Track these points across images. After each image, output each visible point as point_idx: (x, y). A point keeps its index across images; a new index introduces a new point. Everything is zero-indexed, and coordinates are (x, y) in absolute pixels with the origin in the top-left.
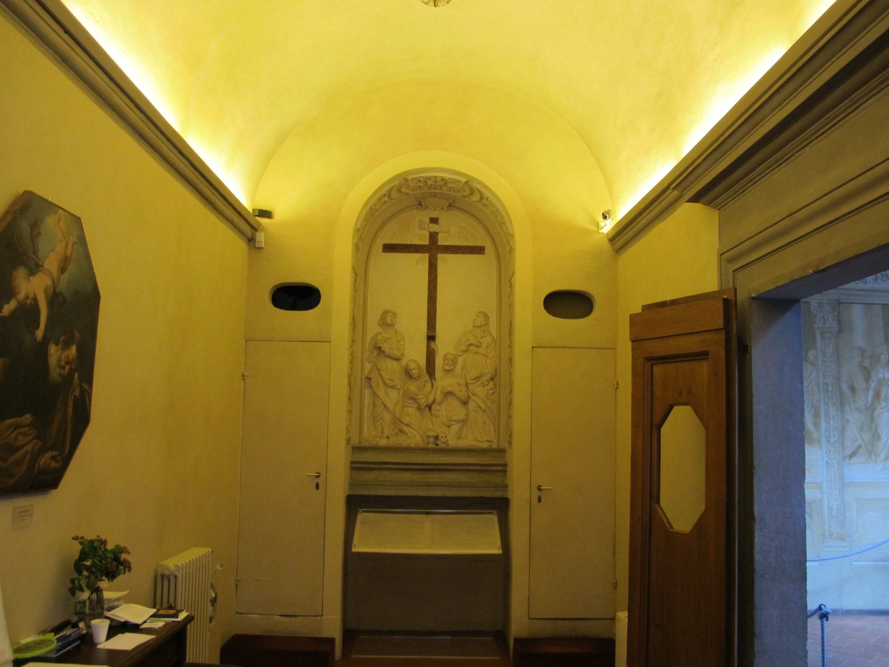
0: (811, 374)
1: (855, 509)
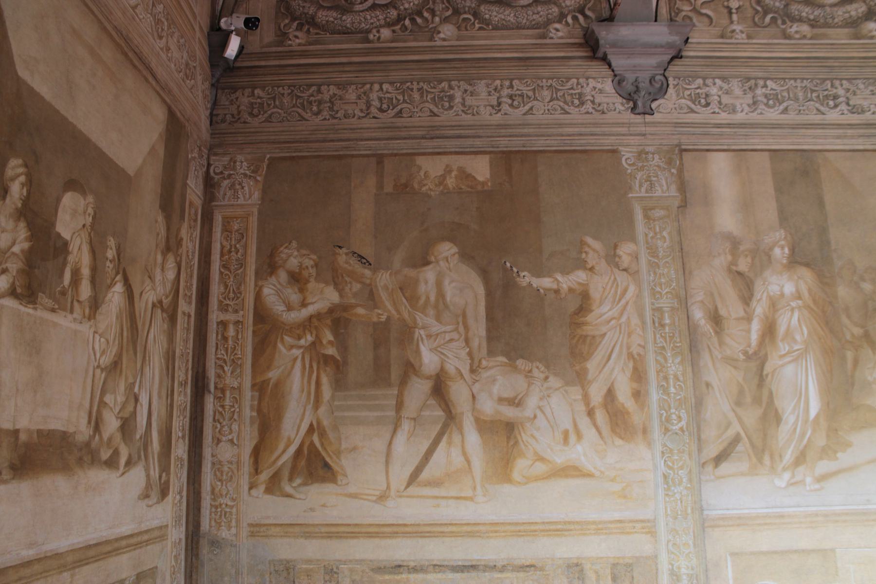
0: (625, 291)
1: (730, 574)
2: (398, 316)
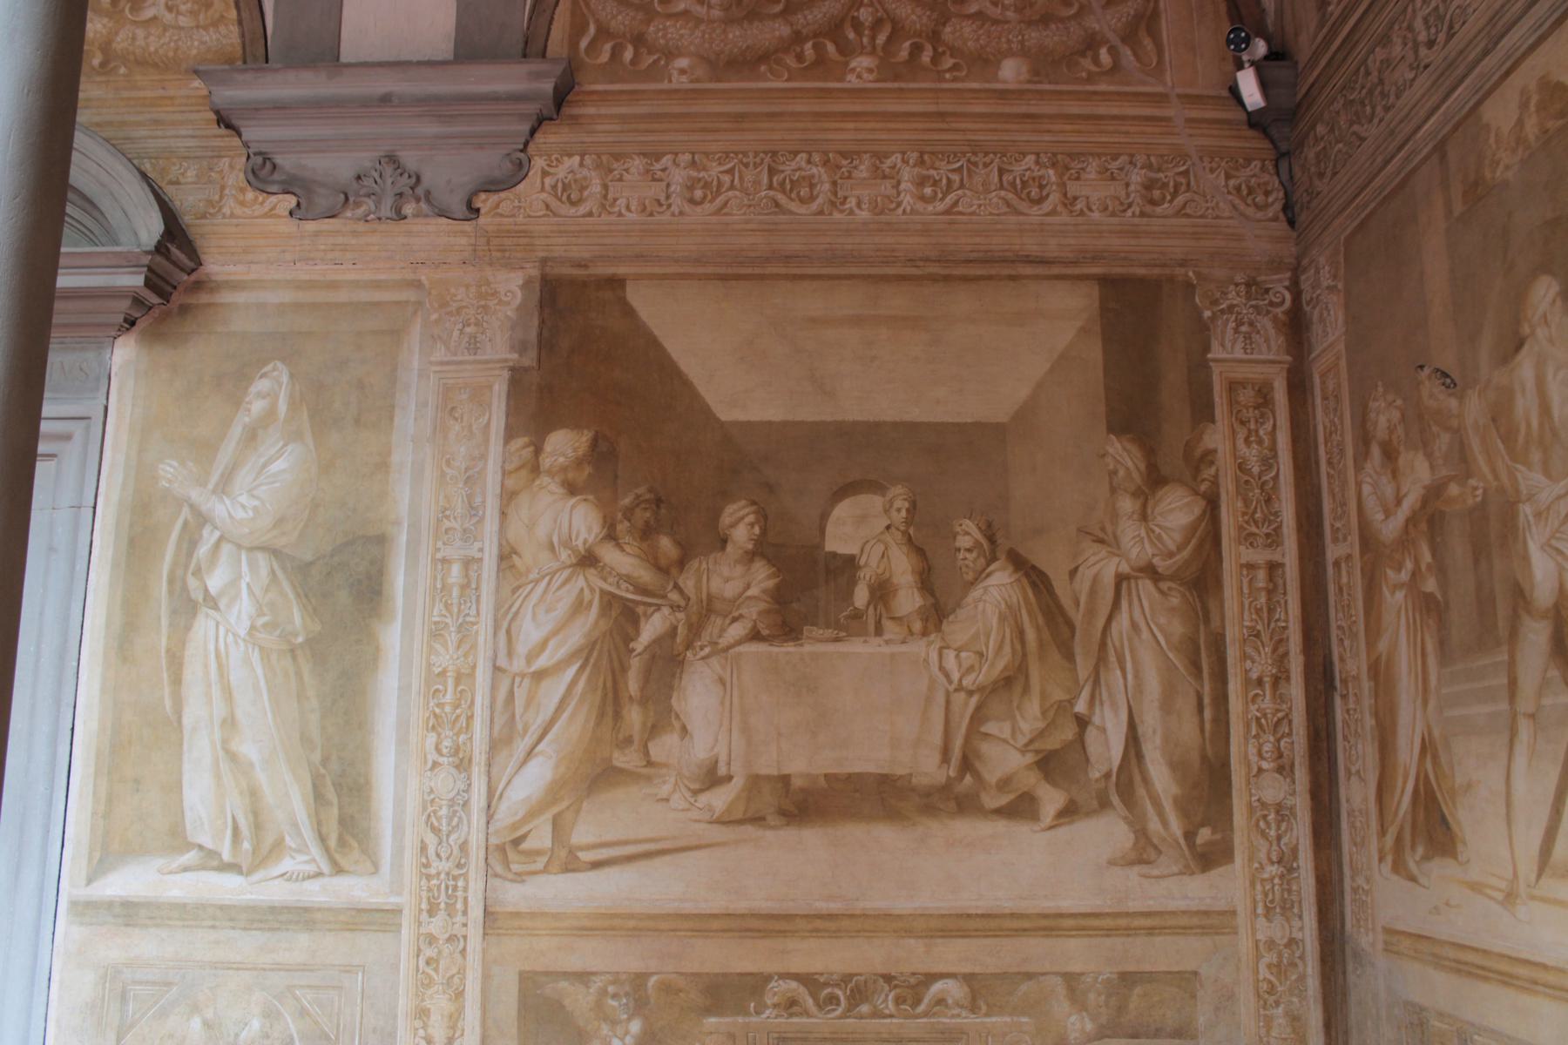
2: (1495, 483)
